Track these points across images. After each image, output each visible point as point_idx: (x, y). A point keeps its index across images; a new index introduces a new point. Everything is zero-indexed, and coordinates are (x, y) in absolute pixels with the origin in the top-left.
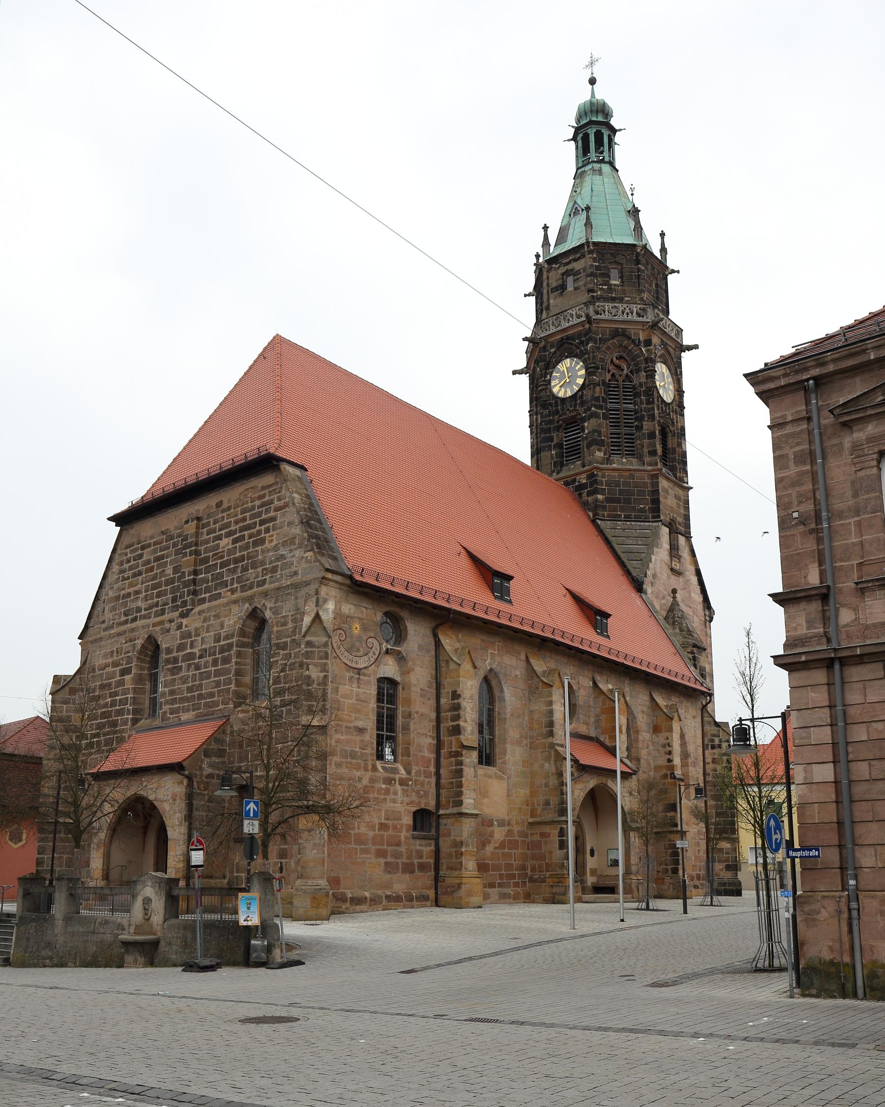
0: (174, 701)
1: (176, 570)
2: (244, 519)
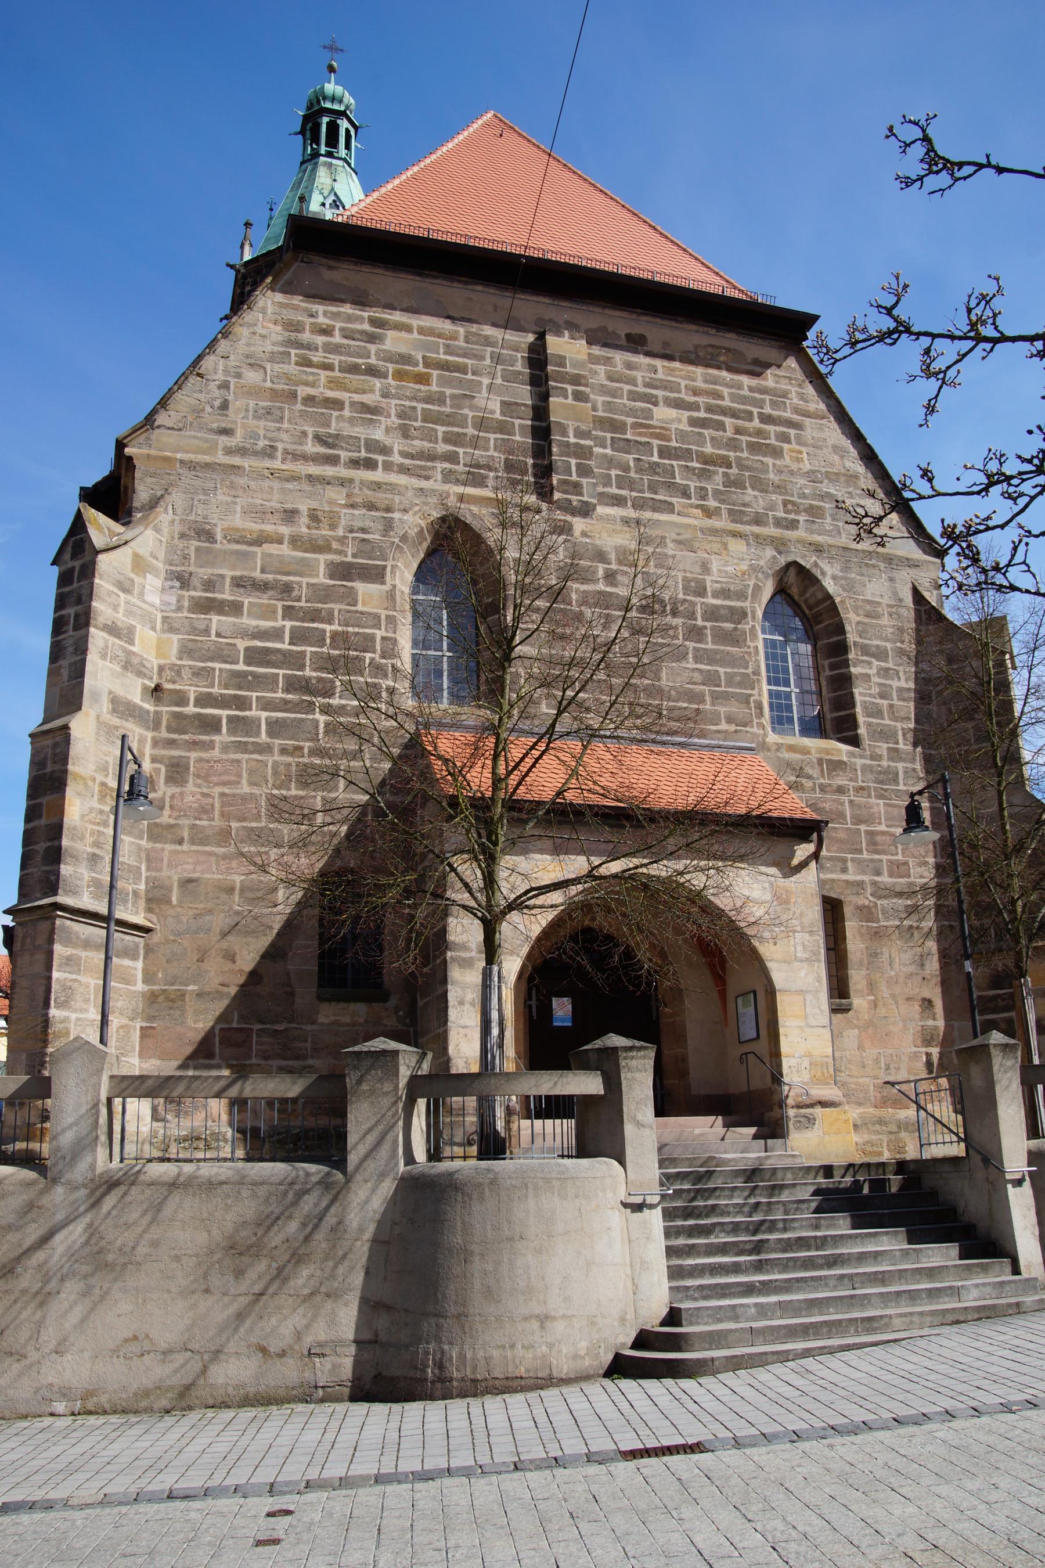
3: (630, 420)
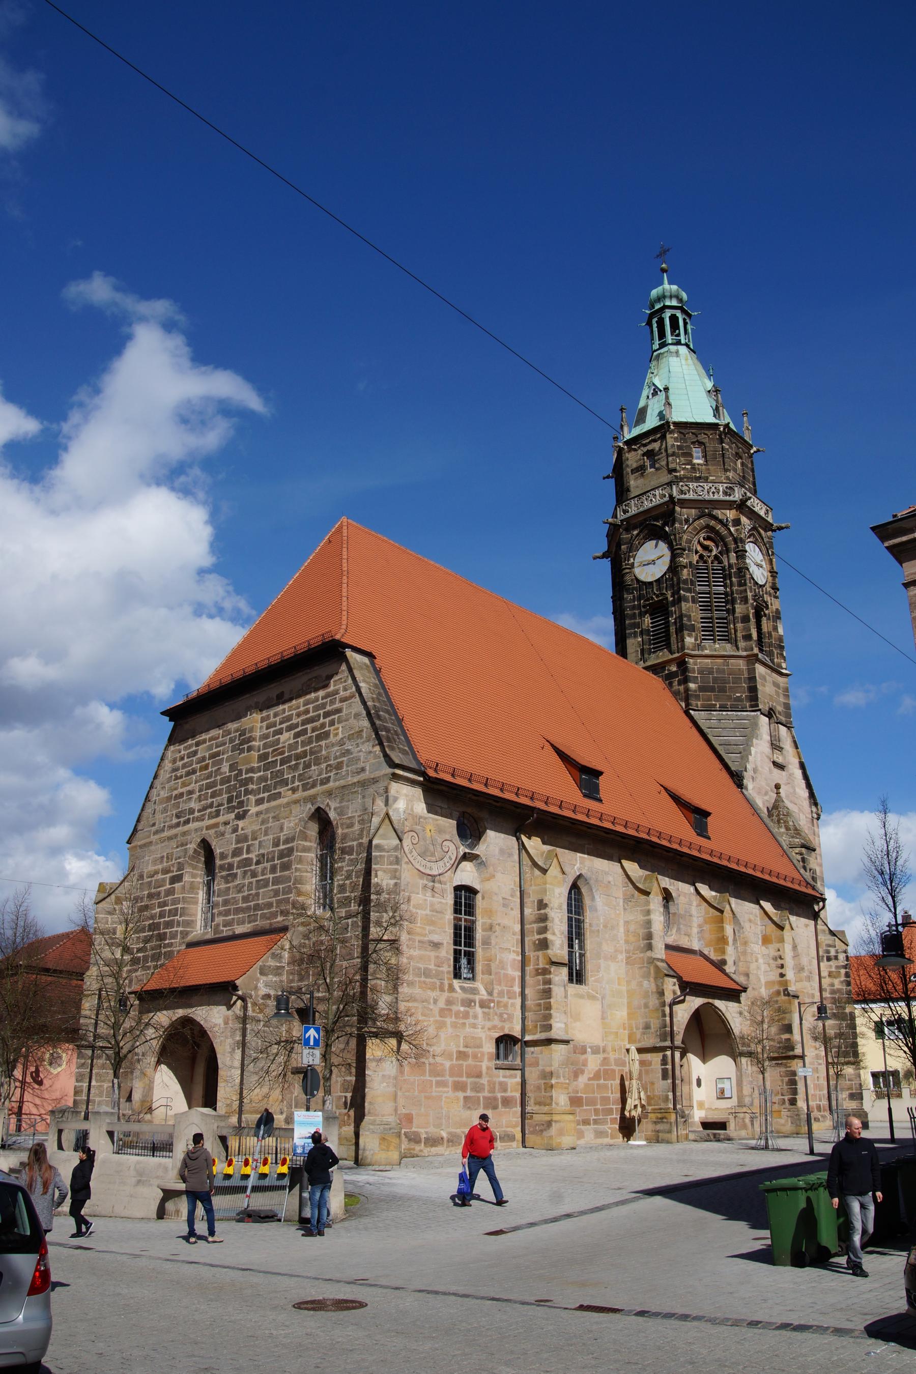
0: (227, 913)
1: (232, 767)
2: (307, 712)
3: (270, 750)
